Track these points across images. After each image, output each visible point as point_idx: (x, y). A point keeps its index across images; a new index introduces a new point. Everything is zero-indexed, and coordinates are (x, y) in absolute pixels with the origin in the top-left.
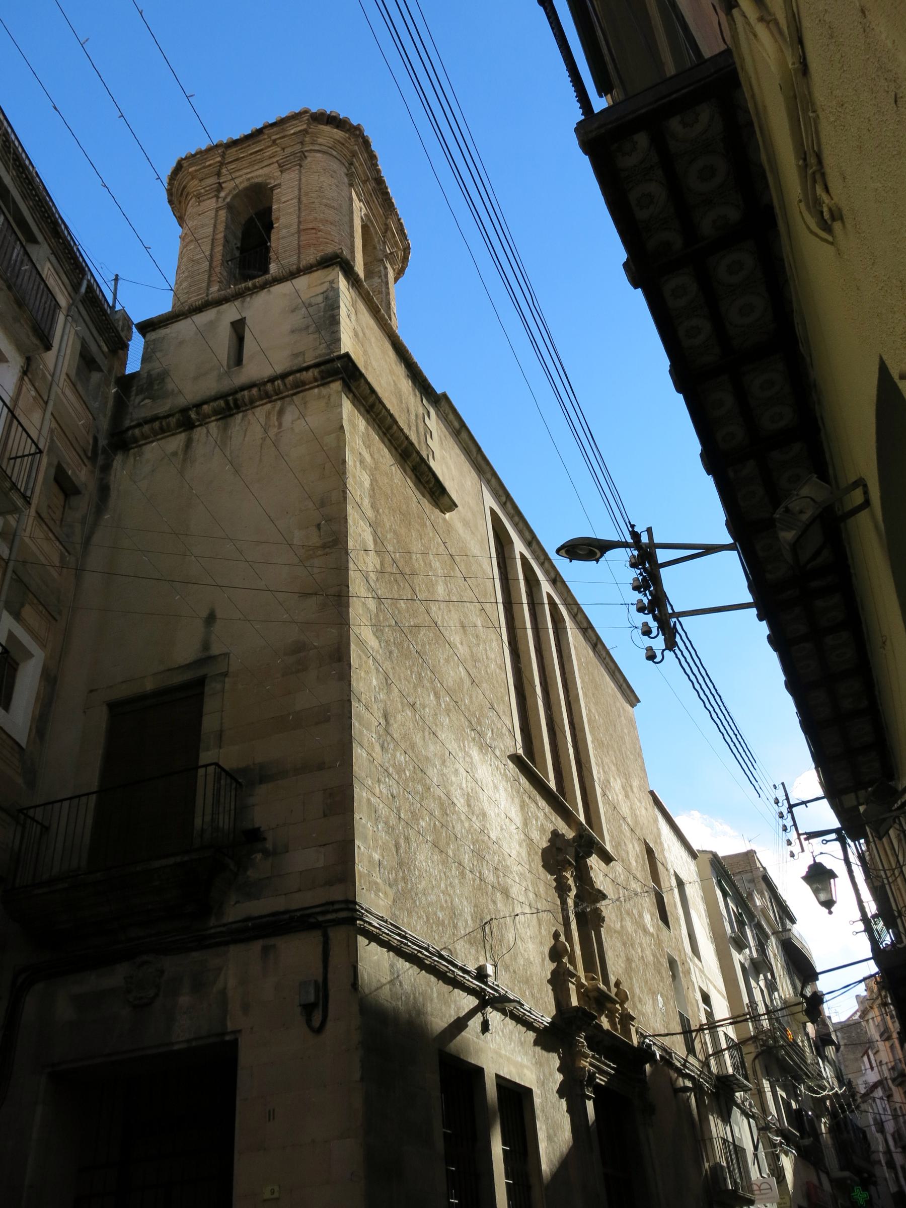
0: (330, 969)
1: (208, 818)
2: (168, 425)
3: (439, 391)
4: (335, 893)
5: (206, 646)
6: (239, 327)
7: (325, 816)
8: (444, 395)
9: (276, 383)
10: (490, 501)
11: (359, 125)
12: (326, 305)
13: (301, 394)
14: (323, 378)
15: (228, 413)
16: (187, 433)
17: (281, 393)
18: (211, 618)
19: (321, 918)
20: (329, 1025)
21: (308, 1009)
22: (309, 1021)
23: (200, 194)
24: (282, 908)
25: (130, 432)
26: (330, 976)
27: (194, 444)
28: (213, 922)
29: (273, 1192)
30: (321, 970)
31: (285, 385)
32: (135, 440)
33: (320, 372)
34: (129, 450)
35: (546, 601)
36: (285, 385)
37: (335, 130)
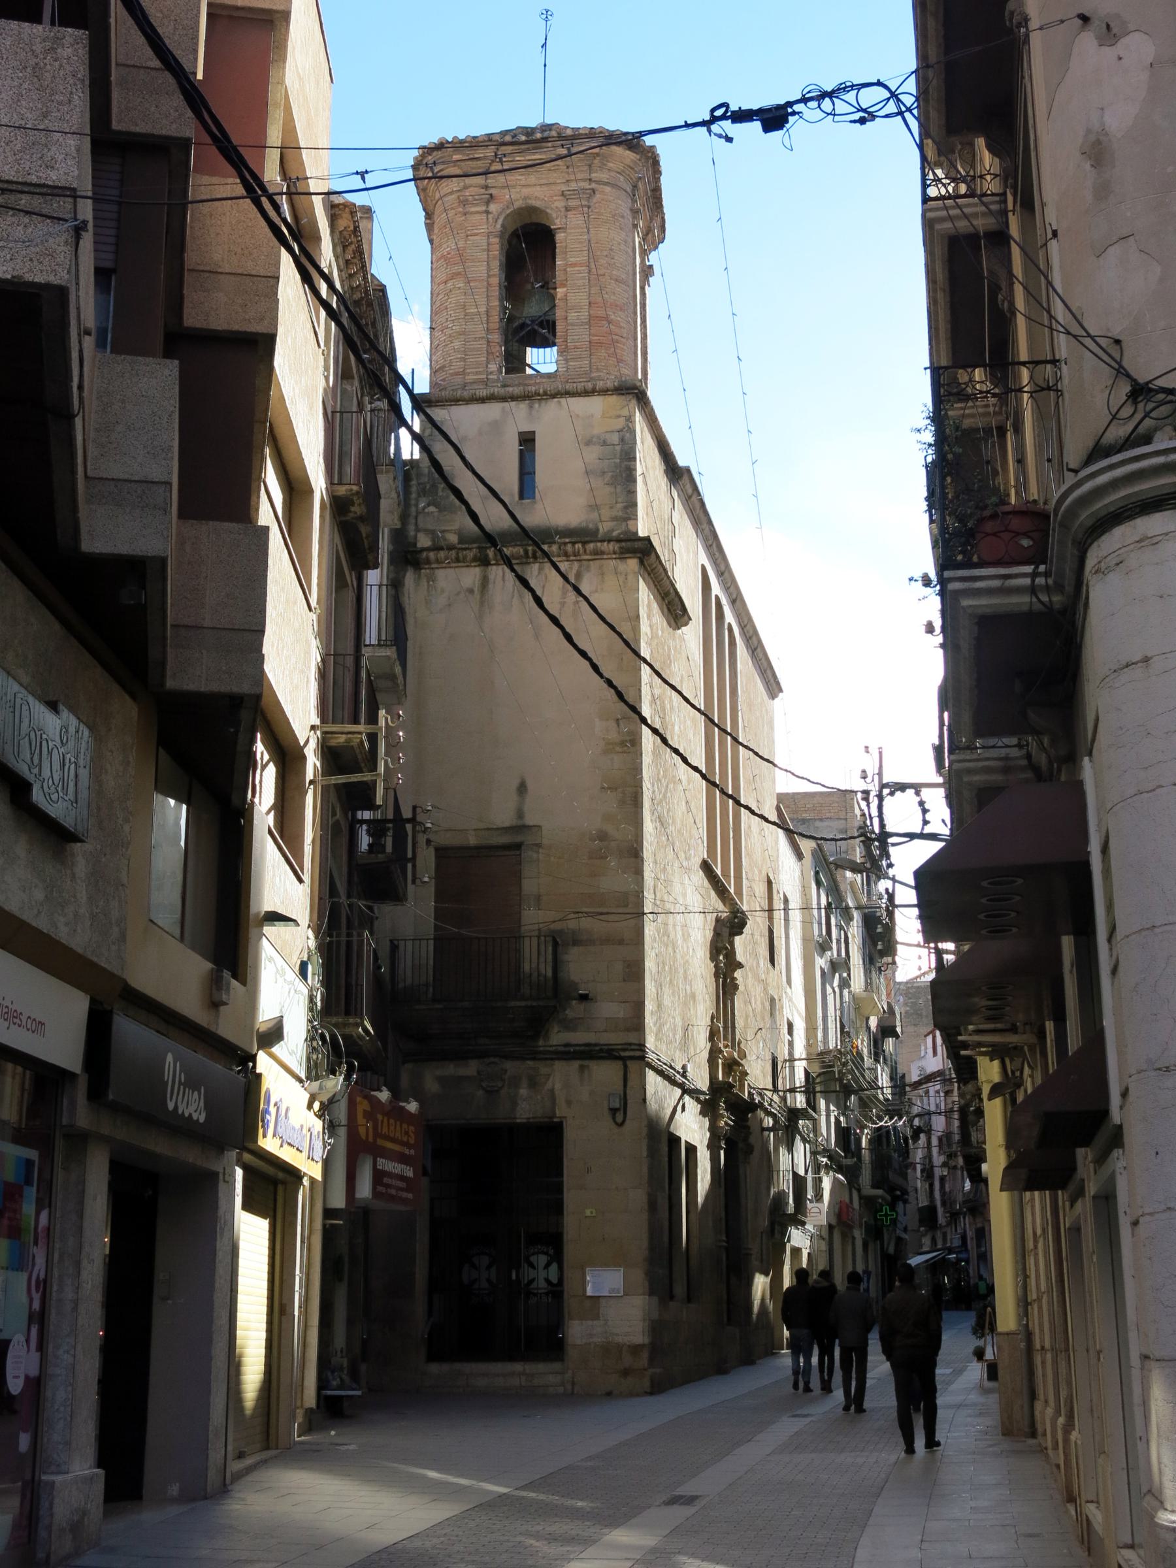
0: (628, 1088)
1: (534, 965)
2: (465, 558)
3: (682, 462)
4: (632, 1038)
5: (520, 814)
6: (527, 441)
7: (624, 980)
8: (688, 470)
9: (577, 546)
10: (703, 559)
11: (653, 147)
12: (622, 450)
13: (598, 561)
14: (622, 553)
15: (524, 560)
16: (482, 568)
17: (579, 555)
18: (522, 788)
19: (623, 1054)
20: (628, 1121)
21: (614, 1111)
22: (614, 1118)
23: (467, 200)
24: (593, 1042)
25: (424, 554)
26: (628, 1092)
27: (491, 586)
28: (541, 1043)
29: (592, 1213)
30: (622, 1088)
31: (585, 551)
32: (428, 562)
33: (621, 548)
34: (421, 569)
35: (726, 627)
36: (585, 551)
37: (628, 152)
